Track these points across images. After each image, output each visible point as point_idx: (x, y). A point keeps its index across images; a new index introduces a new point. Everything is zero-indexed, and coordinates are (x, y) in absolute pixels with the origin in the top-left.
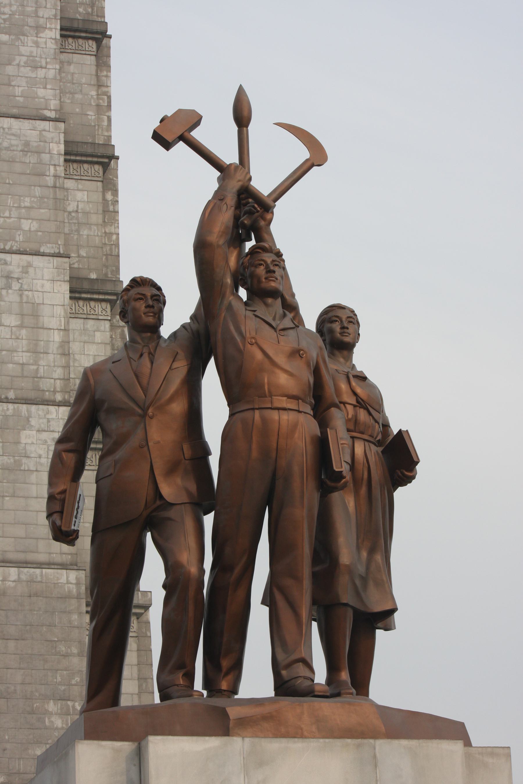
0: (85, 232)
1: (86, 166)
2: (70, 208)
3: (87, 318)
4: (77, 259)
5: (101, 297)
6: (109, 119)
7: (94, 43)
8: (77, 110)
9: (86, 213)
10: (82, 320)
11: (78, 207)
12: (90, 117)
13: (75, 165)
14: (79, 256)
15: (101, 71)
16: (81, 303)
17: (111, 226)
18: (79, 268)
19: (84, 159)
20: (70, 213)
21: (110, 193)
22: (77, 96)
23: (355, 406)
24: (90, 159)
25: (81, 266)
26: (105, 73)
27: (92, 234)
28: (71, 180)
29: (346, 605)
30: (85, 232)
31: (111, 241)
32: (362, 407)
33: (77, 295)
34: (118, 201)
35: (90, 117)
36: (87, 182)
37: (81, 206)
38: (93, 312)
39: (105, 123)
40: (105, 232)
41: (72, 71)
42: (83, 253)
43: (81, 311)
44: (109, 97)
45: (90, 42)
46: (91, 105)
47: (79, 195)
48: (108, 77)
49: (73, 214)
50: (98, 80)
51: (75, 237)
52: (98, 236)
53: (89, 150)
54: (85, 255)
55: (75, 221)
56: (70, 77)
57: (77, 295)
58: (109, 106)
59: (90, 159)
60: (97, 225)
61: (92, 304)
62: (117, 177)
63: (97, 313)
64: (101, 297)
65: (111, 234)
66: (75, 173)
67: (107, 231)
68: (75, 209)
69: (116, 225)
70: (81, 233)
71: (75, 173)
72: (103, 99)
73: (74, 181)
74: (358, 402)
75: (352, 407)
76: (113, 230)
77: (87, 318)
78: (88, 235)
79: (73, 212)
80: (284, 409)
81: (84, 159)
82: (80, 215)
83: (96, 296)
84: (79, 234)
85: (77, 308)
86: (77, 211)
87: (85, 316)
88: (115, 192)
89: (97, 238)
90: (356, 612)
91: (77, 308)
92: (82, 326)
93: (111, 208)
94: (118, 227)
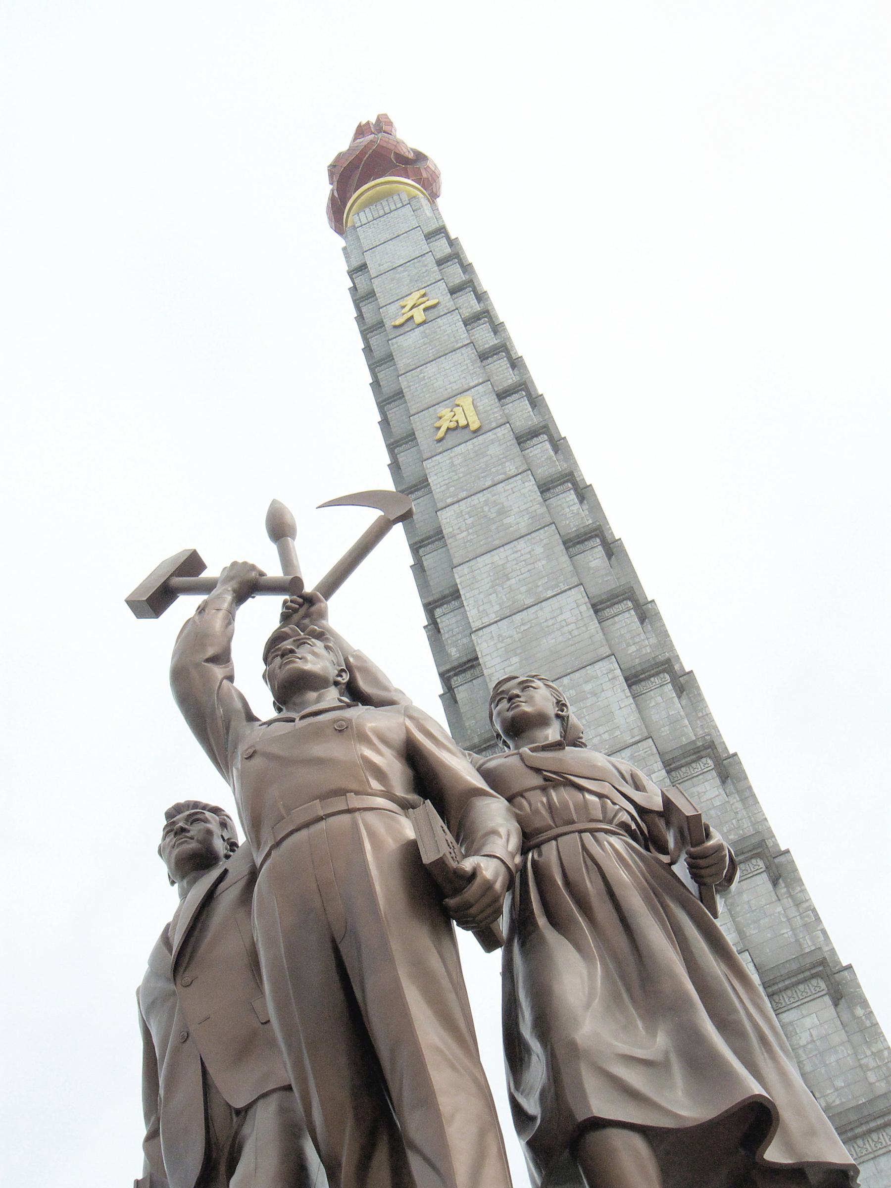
0: (832, 1059)
1: (801, 987)
2: (803, 1042)
3: (875, 1157)
4: (836, 1094)
5: (880, 1122)
6: (824, 932)
7: (758, 860)
8: (769, 935)
9: (823, 1038)
10: (871, 1163)
11: (811, 1036)
12: (786, 935)
13: (789, 992)
14: (836, 1090)
15: (793, 889)
16: (860, 1142)
17: (876, 1043)
18: (842, 1103)
19: (794, 980)
20: (804, 1046)
21: (859, 1008)
22: (762, 922)
23: (544, 789)
24: (801, 976)
25: (844, 1100)
26: (799, 889)
27: (841, 1057)
28: (792, 1011)
29: (599, 1124)
30: (832, 1059)
31: (884, 1060)
32: (556, 785)
33: (850, 1134)
34: (872, 1012)
35: (786, 935)
36: (810, 1003)
37: (814, 1032)
38: (879, 1146)
39: (822, 938)
40: (873, 1053)
41: (746, 900)
42: (839, 1083)
43: (864, 1152)
44: (814, 910)
45: (754, 861)
46: (782, 922)
47: (808, 1022)
48: (804, 891)
49: (810, 1046)
50: (794, 901)
51: (823, 1071)
52: (849, 1055)
53: (794, 967)
54: (843, 1085)
55: (815, 1053)
56: (746, 907)
57: (850, 1134)
58: (818, 919)
59: (801, 976)
60: (842, 1044)
61: (874, 1136)
62: (859, 987)
63: (884, 1144)
64: (880, 1122)
65: (881, 1051)
66: (792, 1000)
67: (874, 1050)
68: (809, 1039)
69: (882, 1039)
70: (828, 1062)
71: (792, 1000)
72: (808, 916)
73: (795, 1010)
74: (546, 779)
75: (538, 792)
76: (881, 1047)
77: (875, 1157)
78: (837, 1061)
79: (808, 1043)
80: (320, 819)
81: (794, 980)
82: (818, 1043)
83: (872, 1125)
84: (826, 1065)
85: (858, 1150)
86: (813, 1041)
87: (872, 1156)
88: (864, 1004)
89: (848, 1058)
90: (642, 1130)
91: (858, 1150)
92: (874, 1169)
93: (868, 1023)
94: (885, 1040)
